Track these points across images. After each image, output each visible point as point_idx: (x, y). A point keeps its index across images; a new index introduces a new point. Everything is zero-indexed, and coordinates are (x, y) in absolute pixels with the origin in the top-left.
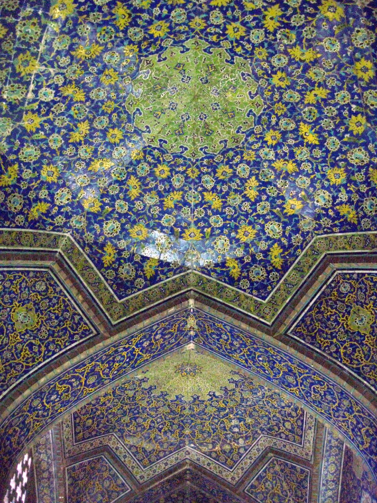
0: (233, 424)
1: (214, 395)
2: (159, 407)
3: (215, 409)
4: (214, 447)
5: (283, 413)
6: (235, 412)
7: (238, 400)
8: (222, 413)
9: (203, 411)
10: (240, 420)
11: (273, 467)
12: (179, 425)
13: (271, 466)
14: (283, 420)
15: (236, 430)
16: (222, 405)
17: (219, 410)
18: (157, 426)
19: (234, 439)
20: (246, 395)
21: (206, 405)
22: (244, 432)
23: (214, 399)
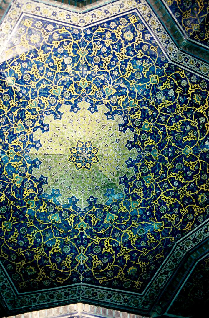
0: (163, 98)
1: (124, 125)
2: (144, 186)
3: (146, 121)
4: (202, 115)
5: (116, 47)
6: (145, 98)
7: (122, 99)
8: (150, 113)
9: (151, 135)
10: (155, 90)
11: (198, 33)
12: (177, 161)
13: (197, 37)
14: (126, 43)
15: (171, 93)
16: (138, 114)
17: (145, 116)
18: (174, 188)
19: (184, 92)
20: (110, 89)
21: (141, 133)
22: (172, 83)
23: (130, 124)
